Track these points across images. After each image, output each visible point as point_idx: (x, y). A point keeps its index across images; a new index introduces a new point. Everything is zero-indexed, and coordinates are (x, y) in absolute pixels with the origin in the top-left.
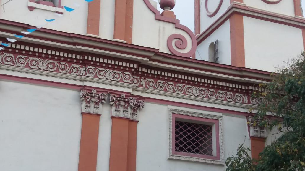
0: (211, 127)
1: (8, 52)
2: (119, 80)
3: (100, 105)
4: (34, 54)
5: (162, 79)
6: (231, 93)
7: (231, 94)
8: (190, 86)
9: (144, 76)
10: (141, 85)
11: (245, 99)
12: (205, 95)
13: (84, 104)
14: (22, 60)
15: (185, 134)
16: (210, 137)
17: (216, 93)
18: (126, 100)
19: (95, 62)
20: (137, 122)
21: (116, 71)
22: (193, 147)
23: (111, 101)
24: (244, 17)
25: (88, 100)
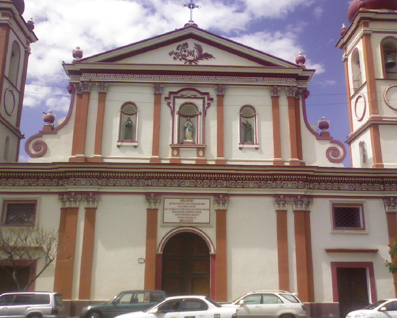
0: (358, 209)
1: (232, 180)
2: (296, 187)
3: (286, 205)
4: (246, 179)
5: (323, 182)
8: (343, 184)
10: (310, 188)
13: (277, 205)
14: (240, 183)
16: (359, 215)
18: (301, 200)
20: (309, 212)
22: (347, 223)
23: (292, 201)
24: (379, 125)
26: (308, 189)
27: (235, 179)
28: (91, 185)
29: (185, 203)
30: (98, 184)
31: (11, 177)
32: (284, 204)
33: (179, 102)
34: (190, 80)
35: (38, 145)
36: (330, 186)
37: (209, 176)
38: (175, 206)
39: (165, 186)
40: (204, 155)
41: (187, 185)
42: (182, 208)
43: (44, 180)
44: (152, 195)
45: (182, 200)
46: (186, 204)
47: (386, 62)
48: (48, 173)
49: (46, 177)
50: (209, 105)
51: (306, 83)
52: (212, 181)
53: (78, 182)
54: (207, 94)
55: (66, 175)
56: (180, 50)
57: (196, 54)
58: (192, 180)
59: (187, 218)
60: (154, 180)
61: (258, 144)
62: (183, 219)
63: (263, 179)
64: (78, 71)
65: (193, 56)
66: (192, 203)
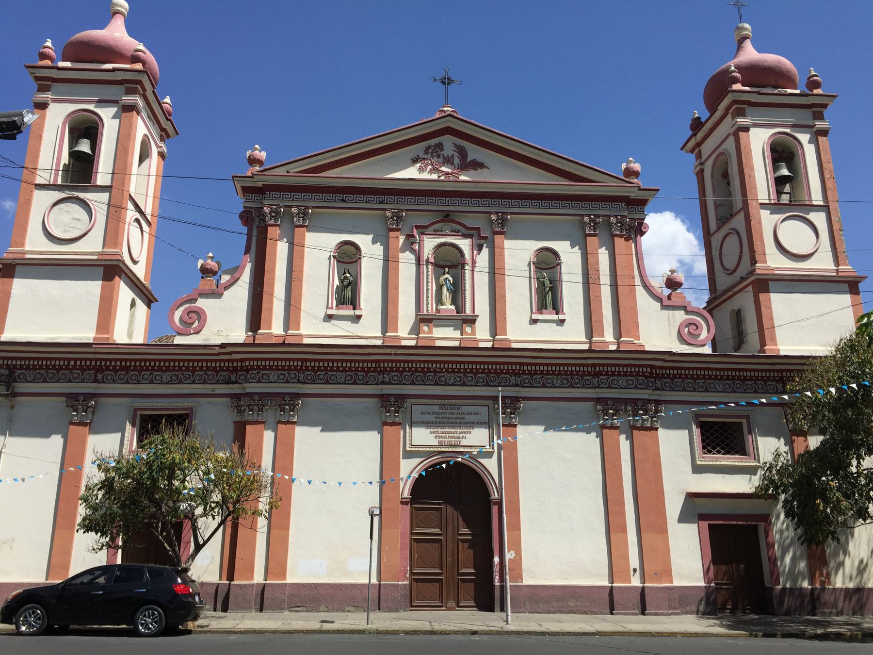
0: (741, 423)
2: (633, 386)
5: (678, 378)
6: (762, 383)
7: (762, 384)
8: (712, 381)
9: (658, 377)
10: (657, 389)
11: (779, 387)
12: (731, 389)
15: (712, 434)
17: (744, 385)
19: (608, 371)
21: (629, 378)
24: (769, 282)
25: (605, 413)
26: (653, 390)
27: (530, 373)
28: (287, 382)
29: (446, 411)
30: (298, 380)
31: (147, 369)
32: (613, 415)
33: (430, 244)
34: (448, 205)
35: (193, 315)
36: (690, 385)
37: (730, 374)
38: (431, 418)
39: (413, 383)
40: (473, 333)
41: (450, 383)
42: (441, 420)
43: (205, 373)
44: (392, 399)
45: (442, 406)
46: (449, 413)
47: (779, 174)
48: (212, 361)
49: (208, 369)
50: (480, 249)
51: (642, 210)
52: (491, 376)
53: (265, 377)
54: (478, 229)
55: (244, 365)
56: (430, 155)
57: (457, 161)
58: (457, 374)
59: (451, 437)
60: (394, 374)
61: (564, 314)
62: (444, 440)
63: (578, 372)
64: (262, 188)
65: (452, 164)
66: (458, 411)
